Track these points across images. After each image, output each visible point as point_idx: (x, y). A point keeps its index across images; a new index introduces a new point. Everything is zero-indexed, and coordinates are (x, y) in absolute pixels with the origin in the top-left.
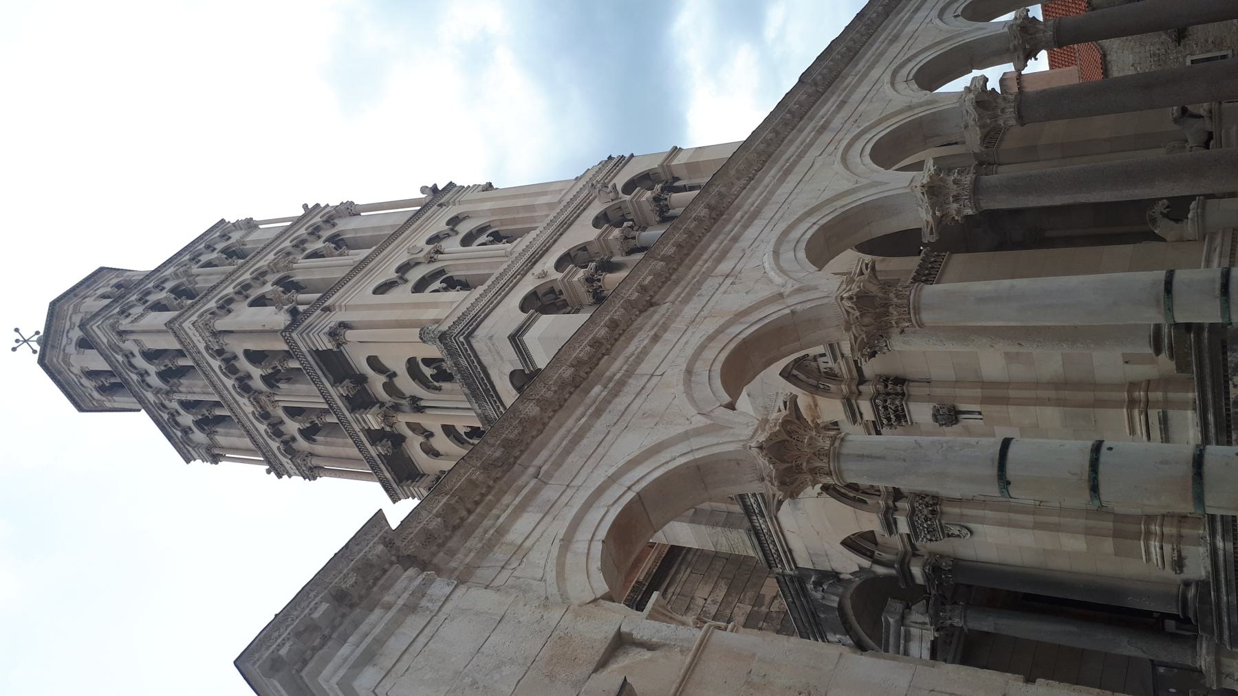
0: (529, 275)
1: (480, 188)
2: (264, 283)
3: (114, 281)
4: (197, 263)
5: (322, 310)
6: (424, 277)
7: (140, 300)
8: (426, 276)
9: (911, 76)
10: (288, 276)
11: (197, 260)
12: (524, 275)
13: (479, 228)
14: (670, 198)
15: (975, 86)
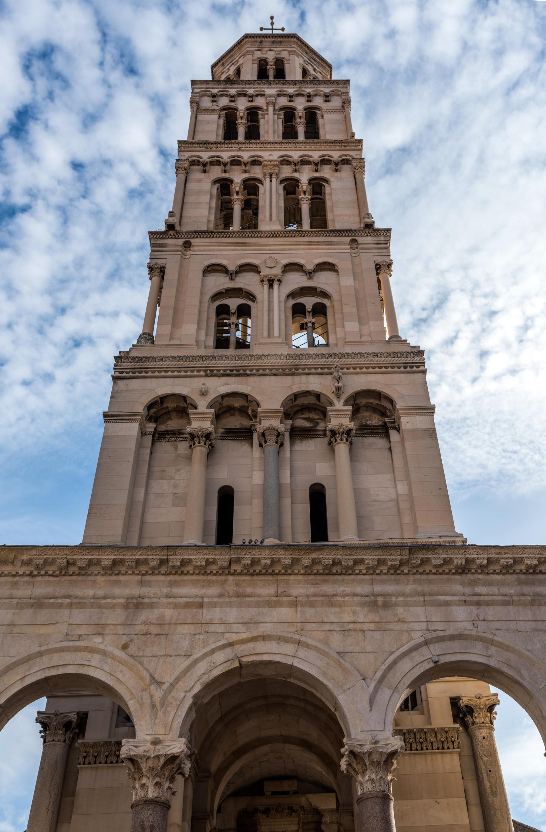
0: (203, 380)
1: (379, 260)
2: (246, 172)
3: (284, 54)
4: (290, 101)
5: (185, 243)
6: (240, 290)
7: (232, 97)
8: (243, 290)
9: (245, 660)
10: (262, 181)
11: (292, 99)
12: (206, 376)
13: (324, 291)
14: (338, 443)
15: (169, 746)
